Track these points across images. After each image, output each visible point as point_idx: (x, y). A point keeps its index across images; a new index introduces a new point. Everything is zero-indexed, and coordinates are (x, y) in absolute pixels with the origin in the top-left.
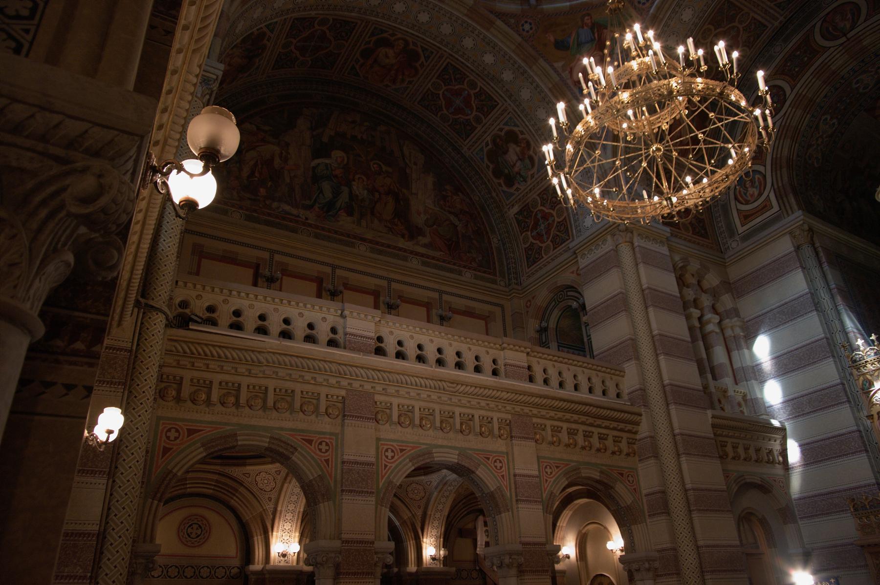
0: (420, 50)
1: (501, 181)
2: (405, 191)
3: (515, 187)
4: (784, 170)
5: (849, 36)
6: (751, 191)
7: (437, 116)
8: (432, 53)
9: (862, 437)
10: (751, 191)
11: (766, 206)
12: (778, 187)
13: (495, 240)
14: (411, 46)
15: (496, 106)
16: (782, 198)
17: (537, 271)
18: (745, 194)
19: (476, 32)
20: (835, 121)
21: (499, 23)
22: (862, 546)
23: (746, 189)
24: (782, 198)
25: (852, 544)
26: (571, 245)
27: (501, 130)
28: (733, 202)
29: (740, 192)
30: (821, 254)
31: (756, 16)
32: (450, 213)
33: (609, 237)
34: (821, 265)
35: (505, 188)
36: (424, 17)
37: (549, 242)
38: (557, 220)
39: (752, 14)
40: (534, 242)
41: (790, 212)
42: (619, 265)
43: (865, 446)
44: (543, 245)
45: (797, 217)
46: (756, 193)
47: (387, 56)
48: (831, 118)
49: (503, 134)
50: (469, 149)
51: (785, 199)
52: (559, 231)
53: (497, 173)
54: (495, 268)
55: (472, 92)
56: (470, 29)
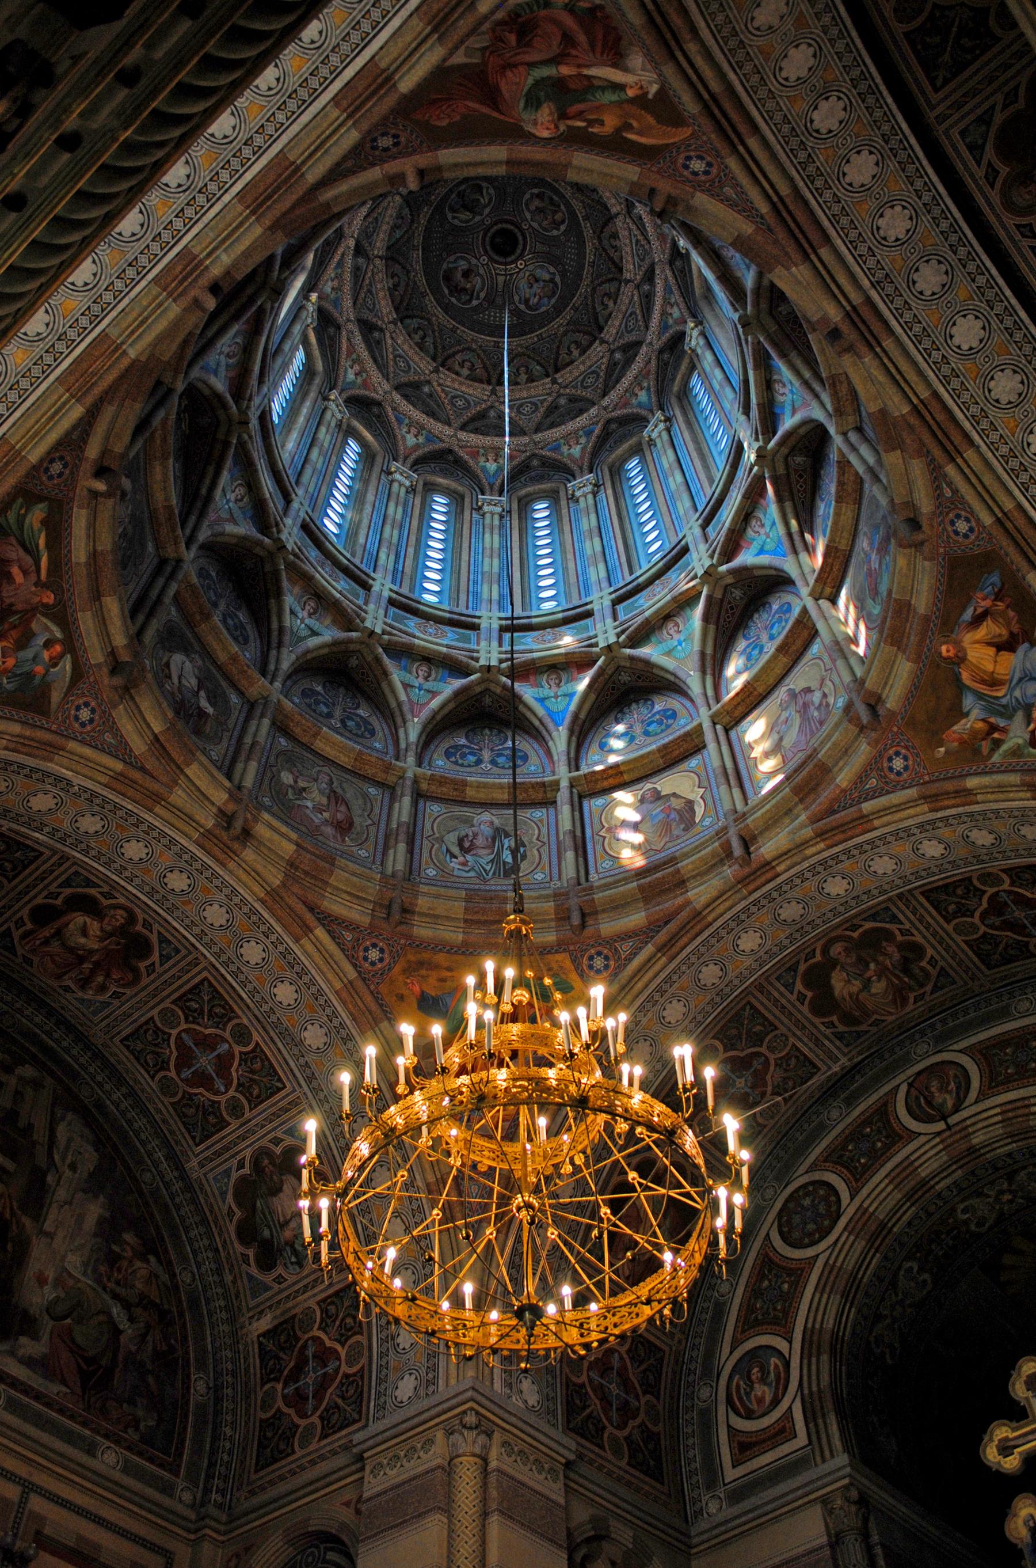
0: (154, 939)
1: (251, 1253)
2: (27, 1221)
3: (275, 1274)
4: (825, 1358)
5: (953, 1120)
6: (759, 1389)
7: (153, 1078)
8: (178, 951)
10: (759, 1389)
11: (783, 1430)
12: (811, 1393)
13: (201, 1386)
14: (139, 927)
15: (279, 1090)
16: (815, 1420)
17: (272, 1483)
18: (748, 1394)
19: (273, 938)
20: (926, 1276)
21: (320, 932)
26: (358, 1437)
27: (277, 1141)
28: (722, 1408)
29: (738, 1386)
31: (799, 1045)
32: (115, 1296)
33: (440, 1435)
35: (254, 1271)
36: (178, 882)
37: (315, 1419)
38: (344, 1368)
39: (792, 1040)
40: (285, 1410)
41: (827, 1453)
42: (448, 1509)
44: (302, 1423)
46: (768, 1399)
47: (84, 932)
48: (921, 1270)
49: (278, 1150)
50: (201, 1165)
51: (820, 1421)
52: (343, 1398)
53: (247, 1233)
54: (181, 1455)
55: (237, 1049)
56: (263, 928)
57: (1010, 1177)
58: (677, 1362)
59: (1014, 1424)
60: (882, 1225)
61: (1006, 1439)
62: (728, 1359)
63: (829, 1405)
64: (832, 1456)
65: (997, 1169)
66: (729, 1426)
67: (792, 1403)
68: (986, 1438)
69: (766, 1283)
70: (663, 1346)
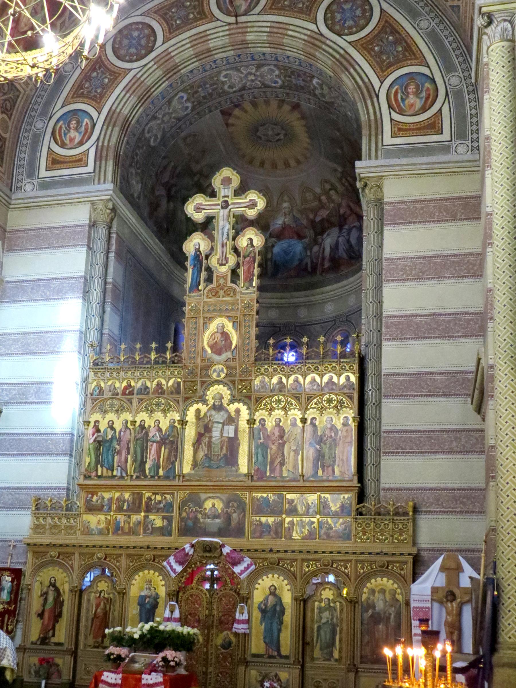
4: (117, 129)
6: (73, 134)
9: (72, 441)
10: (73, 134)
11: (80, 160)
16: (101, 161)
18: (65, 134)
22: (28, 544)
23: (69, 129)
24: (101, 161)
25: (21, 541)
29: (61, 127)
30: (114, 241)
34: (108, 252)
43: (71, 451)
45: (106, 189)
46: (77, 140)
51: (103, 162)
57: (259, 67)
58: (26, 100)
59: (208, 198)
60: (176, 66)
61: (201, 204)
62: (59, 110)
63: (111, 155)
64: (104, 182)
65: (253, 60)
66: (49, 148)
67: (90, 147)
68: (191, 200)
69: (95, 74)
70: (21, 90)
